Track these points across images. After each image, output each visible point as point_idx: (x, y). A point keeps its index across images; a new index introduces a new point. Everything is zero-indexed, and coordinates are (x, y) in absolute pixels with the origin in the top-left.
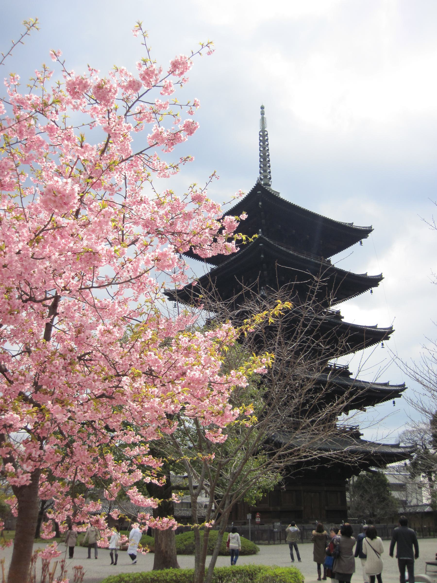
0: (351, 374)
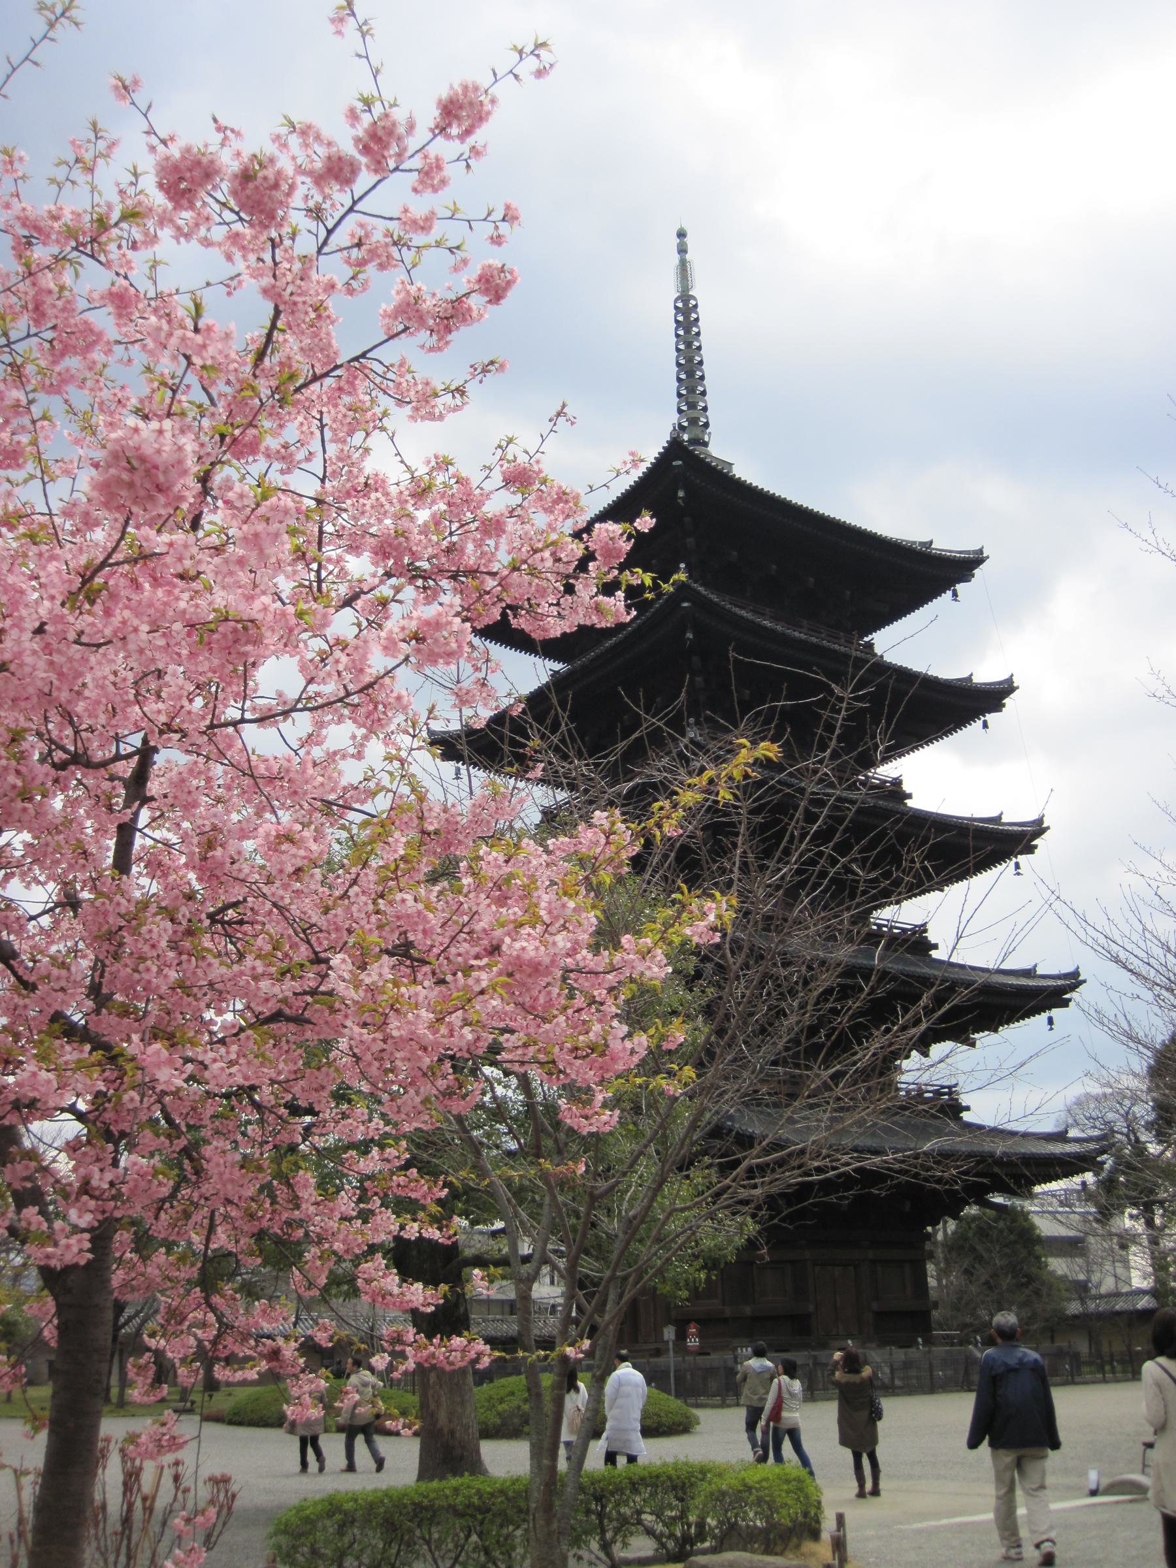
0: (935, 947)
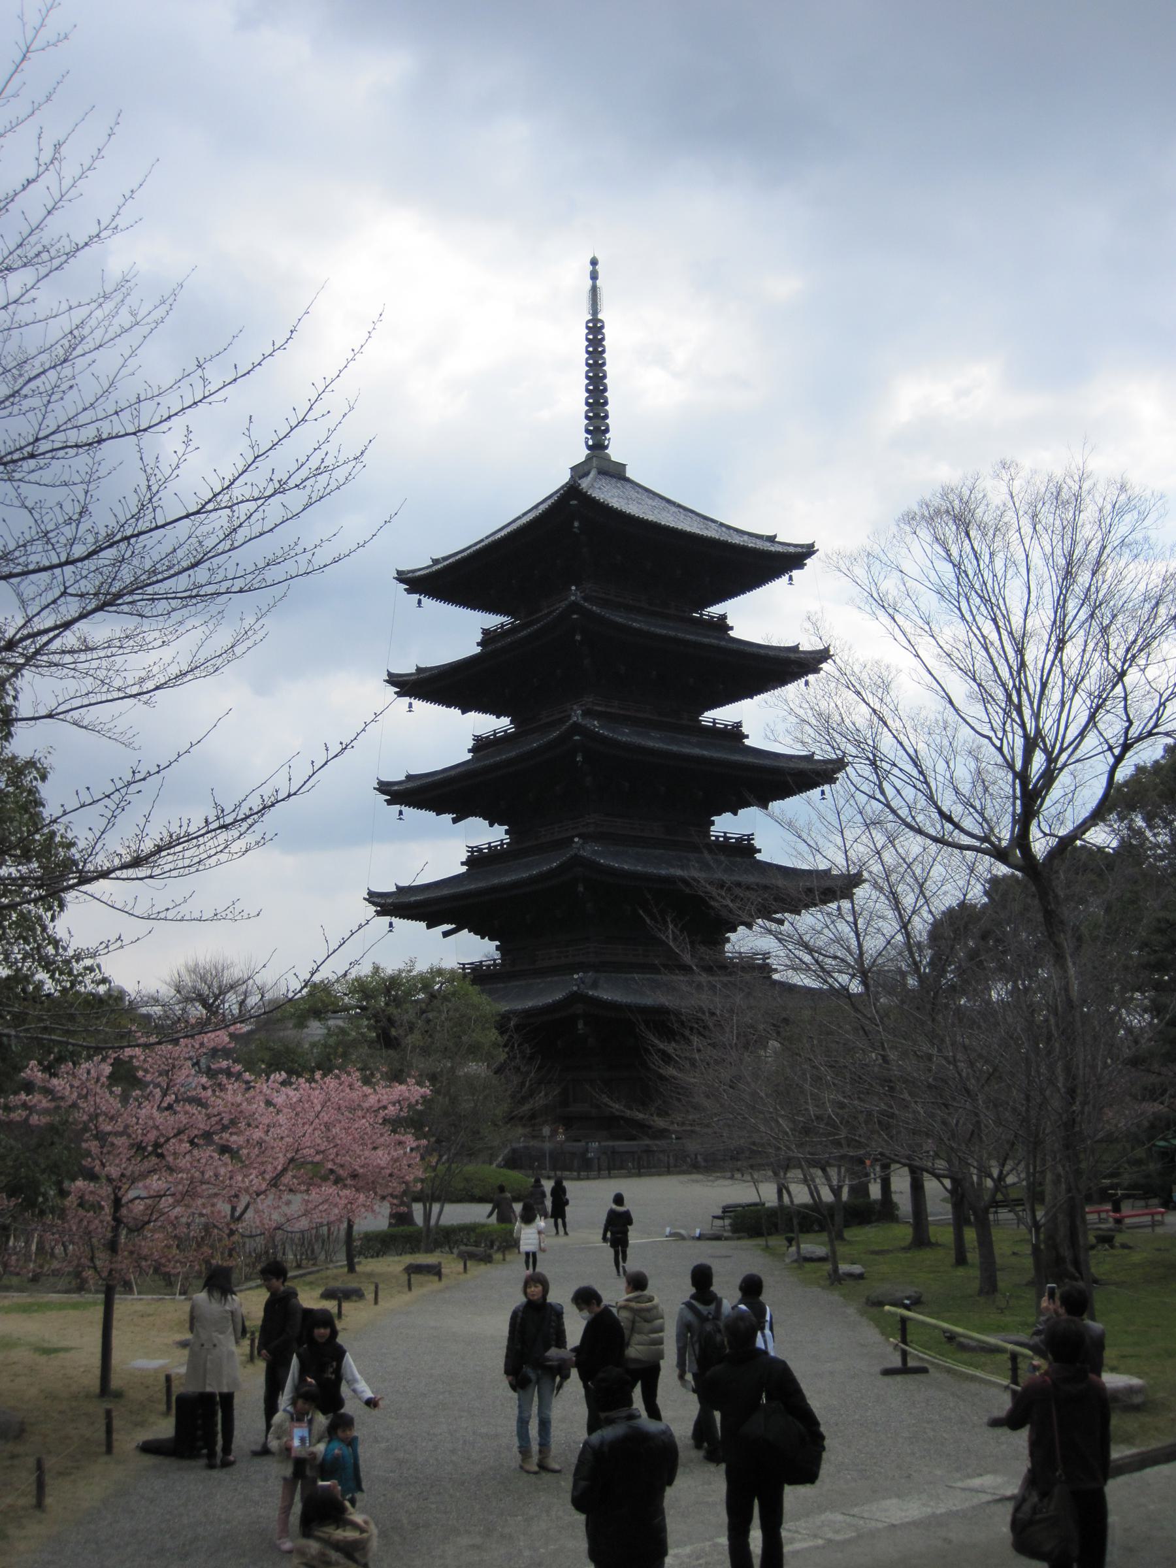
0: (759, 851)
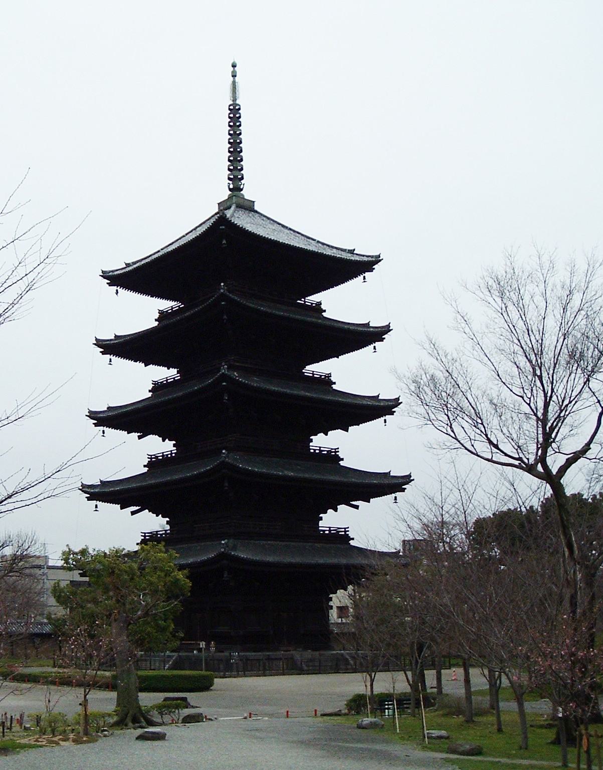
0: (342, 459)
